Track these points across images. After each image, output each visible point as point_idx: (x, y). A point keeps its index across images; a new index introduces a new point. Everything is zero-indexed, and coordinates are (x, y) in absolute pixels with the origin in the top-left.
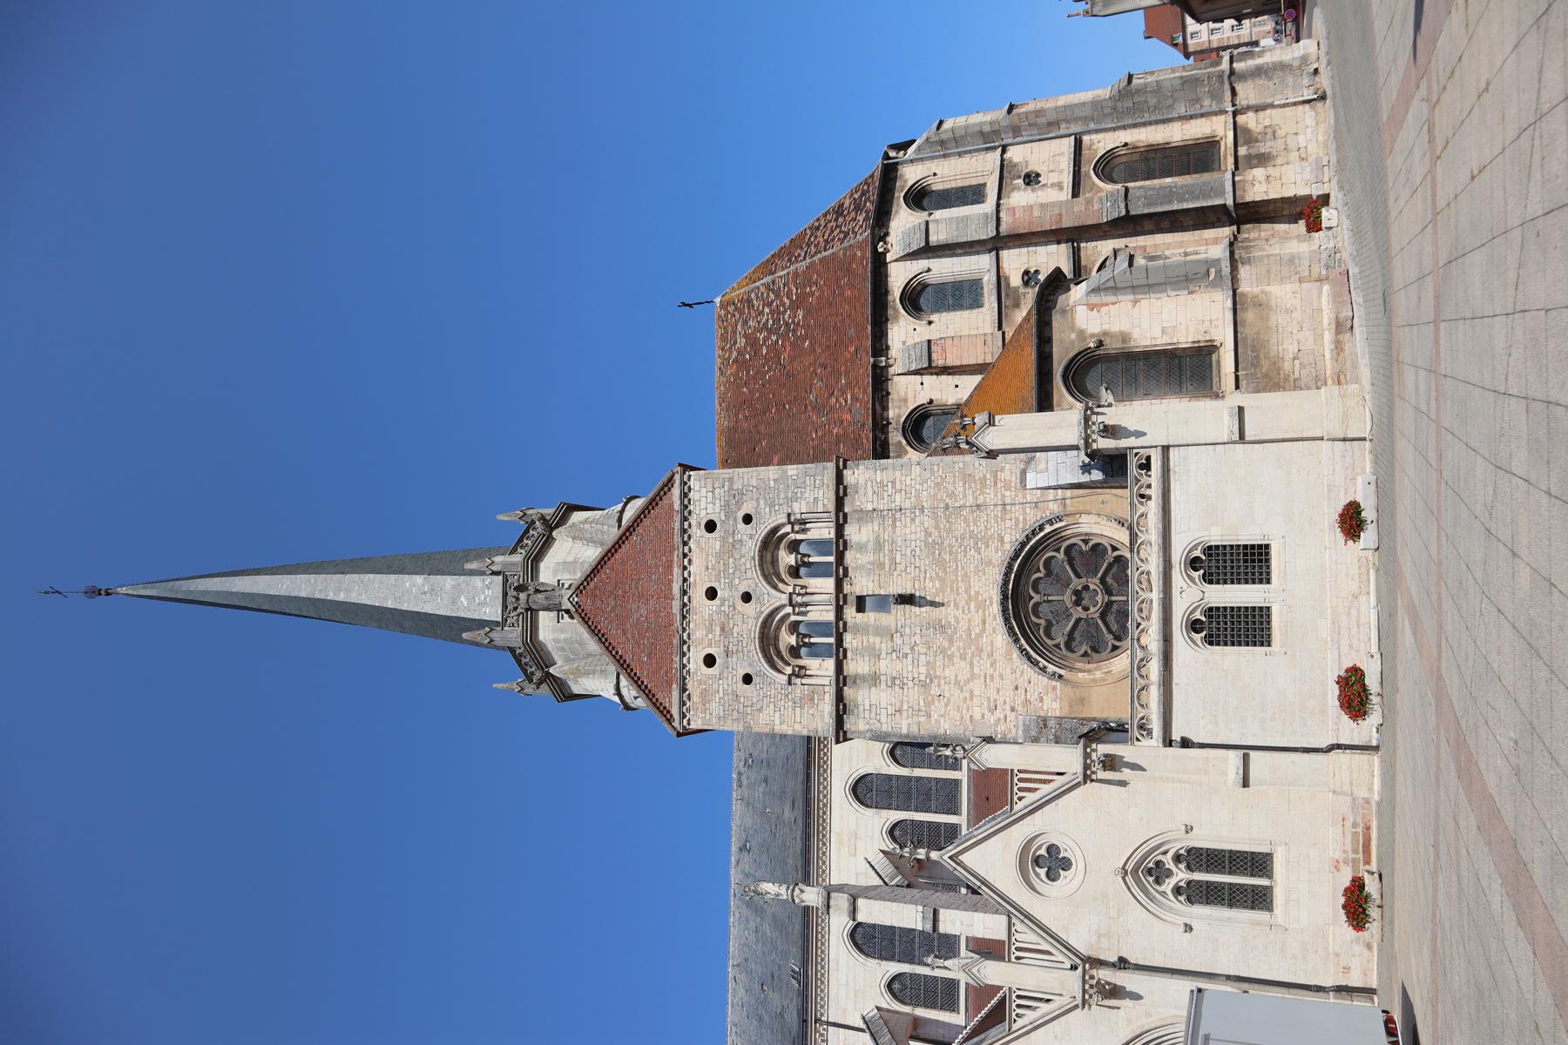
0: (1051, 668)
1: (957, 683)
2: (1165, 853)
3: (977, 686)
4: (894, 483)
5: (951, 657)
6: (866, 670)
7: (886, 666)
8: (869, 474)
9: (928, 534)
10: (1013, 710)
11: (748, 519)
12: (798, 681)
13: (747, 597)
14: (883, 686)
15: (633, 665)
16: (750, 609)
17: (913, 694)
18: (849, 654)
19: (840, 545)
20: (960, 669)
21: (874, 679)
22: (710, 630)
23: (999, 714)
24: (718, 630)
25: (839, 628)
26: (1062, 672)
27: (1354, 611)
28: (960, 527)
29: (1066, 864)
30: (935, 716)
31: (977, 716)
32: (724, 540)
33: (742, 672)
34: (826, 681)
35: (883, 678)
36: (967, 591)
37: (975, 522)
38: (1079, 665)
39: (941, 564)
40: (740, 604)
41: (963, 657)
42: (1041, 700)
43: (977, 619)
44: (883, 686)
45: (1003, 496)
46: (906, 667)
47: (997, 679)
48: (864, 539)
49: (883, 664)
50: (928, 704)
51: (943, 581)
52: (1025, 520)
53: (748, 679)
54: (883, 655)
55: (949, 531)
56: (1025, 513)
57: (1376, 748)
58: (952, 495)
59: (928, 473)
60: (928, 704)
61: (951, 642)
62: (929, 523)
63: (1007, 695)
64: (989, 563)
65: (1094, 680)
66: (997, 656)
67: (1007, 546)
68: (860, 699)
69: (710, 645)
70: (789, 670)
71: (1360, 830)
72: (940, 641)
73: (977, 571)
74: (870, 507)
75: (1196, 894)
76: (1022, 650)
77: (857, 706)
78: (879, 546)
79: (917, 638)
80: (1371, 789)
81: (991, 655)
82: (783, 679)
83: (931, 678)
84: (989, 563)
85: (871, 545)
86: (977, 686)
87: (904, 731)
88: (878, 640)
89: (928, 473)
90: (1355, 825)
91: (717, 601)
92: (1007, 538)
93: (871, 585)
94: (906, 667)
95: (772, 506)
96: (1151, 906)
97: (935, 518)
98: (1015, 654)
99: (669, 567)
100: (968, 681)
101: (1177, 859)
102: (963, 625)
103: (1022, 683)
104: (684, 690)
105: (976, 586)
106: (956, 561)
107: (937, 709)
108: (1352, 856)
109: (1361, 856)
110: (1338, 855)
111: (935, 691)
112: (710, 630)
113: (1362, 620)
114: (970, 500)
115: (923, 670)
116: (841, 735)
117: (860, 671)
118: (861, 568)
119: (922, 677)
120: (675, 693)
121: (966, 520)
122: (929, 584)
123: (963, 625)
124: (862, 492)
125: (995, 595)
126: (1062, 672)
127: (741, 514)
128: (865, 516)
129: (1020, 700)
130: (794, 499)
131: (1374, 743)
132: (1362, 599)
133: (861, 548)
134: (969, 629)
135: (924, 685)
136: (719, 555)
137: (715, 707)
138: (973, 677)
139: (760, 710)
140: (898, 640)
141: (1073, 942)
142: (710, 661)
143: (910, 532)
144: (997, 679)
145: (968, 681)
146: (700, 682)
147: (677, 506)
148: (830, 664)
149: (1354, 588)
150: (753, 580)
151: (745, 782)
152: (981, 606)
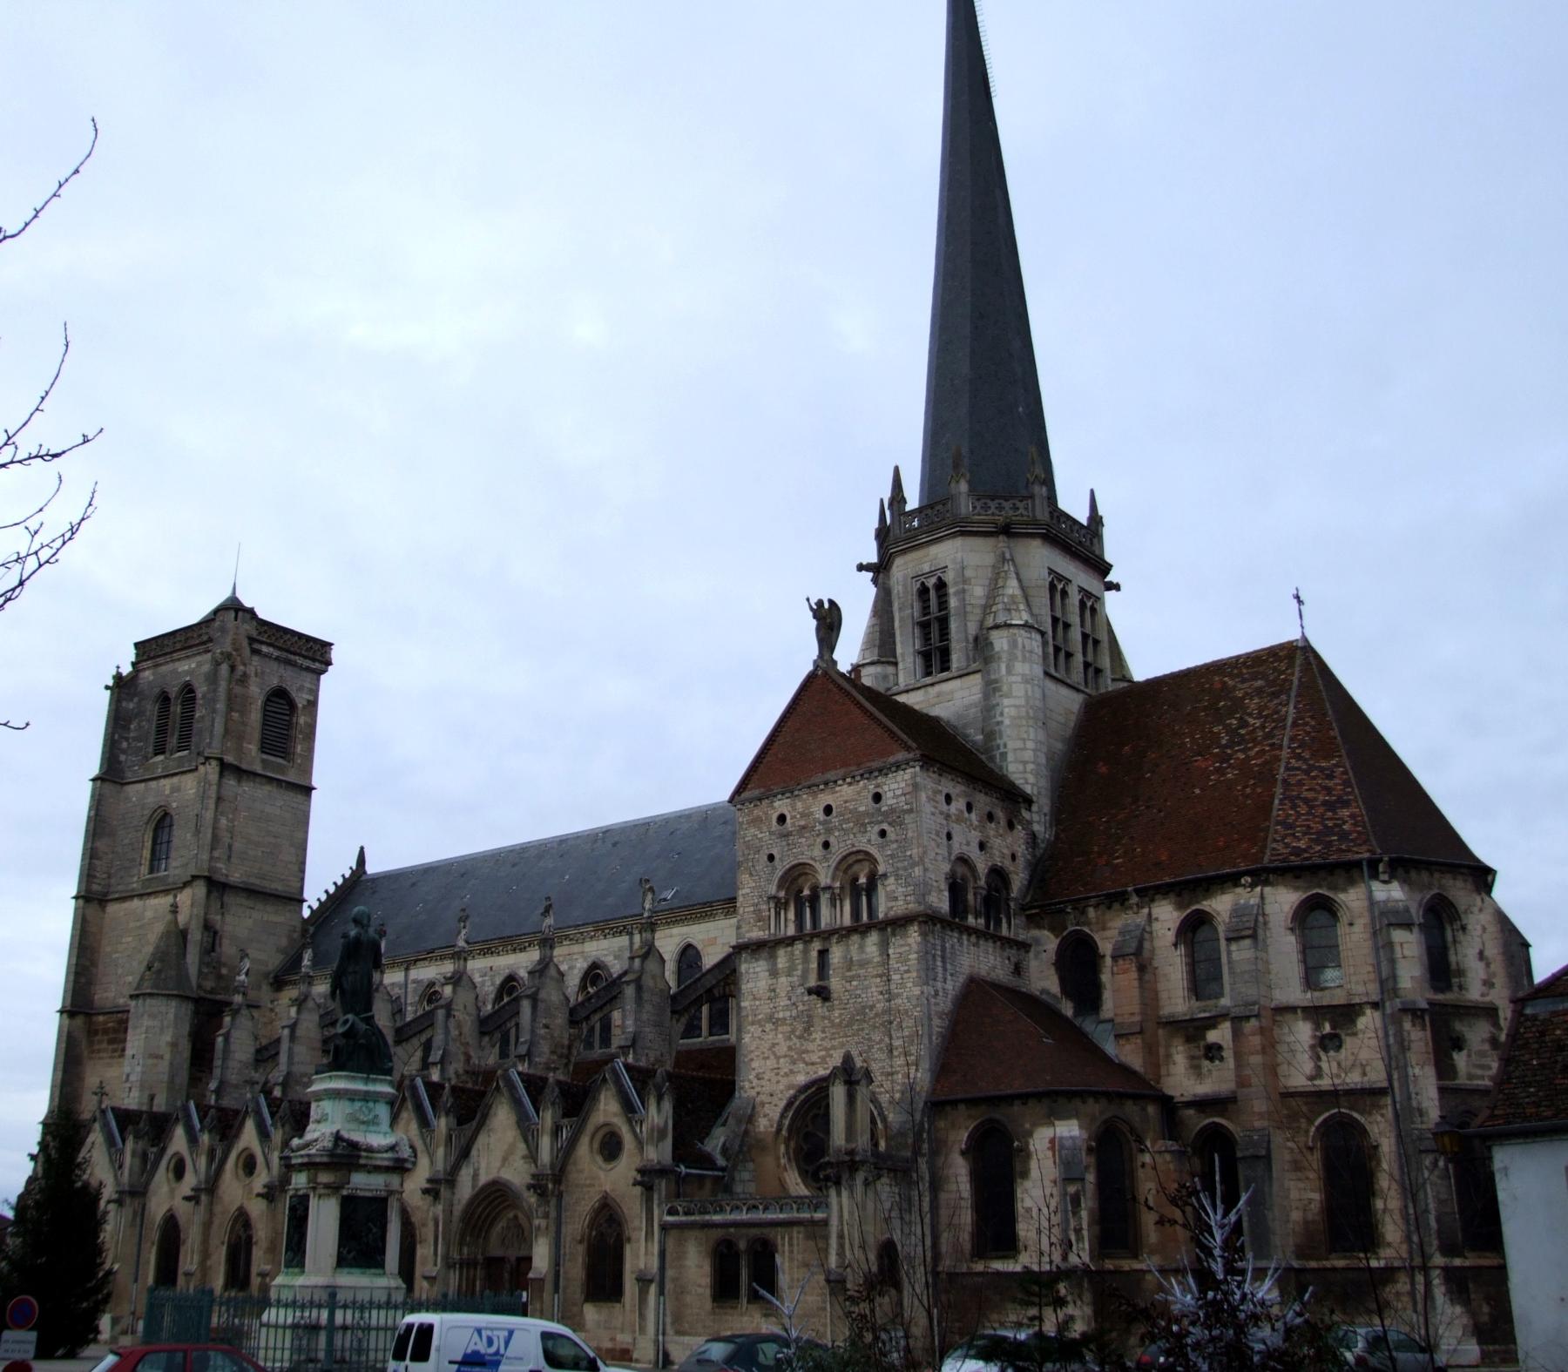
1: (774, 1045)
3: (771, 1063)
4: (908, 971)
5: (790, 1039)
9: (872, 1007)
11: (883, 834)
12: (772, 905)
13: (826, 845)
16: (818, 851)
17: (766, 1009)
21: (774, 973)
23: (755, 1082)
30: (752, 1029)
32: (866, 814)
33: (775, 852)
36: (834, 1048)
37: (880, 1049)
38: (792, 1144)
39: (850, 1025)
40: (820, 840)
41: (790, 1048)
43: (815, 1058)
49: (783, 980)
53: (771, 858)
60: (759, 1022)
61: (799, 1037)
62: (880, 1006)
63: (768, 1088)
65: (778, 1159)
66: (791, 1078)
70: (782, 894)
72: (800, 1028)
76: (795, 1097)
78: (863, 964)
79: (801, 1008)
81: (792, 1071)
82: (773, 890)
83: (776, 1023)
95: (892, 856)
97: (884, 1012)
98: (792, 1092)
102: (811, 1047)
103: (775, 1100)
111: (769, 1027)
112: (803, 815)
114: (896, 1043)
115: (781, 1015)
118: (848, 951)
121: (881, 1041)
123: (811, 1047)
128: (884, 946)
130: (898, 877)
133: (862, 948)
134: (807, 1052)
135: (770, 1018)
138: (778, 1058)
148: (791, 931)
150: (839, 849)
152: (823, 1059)
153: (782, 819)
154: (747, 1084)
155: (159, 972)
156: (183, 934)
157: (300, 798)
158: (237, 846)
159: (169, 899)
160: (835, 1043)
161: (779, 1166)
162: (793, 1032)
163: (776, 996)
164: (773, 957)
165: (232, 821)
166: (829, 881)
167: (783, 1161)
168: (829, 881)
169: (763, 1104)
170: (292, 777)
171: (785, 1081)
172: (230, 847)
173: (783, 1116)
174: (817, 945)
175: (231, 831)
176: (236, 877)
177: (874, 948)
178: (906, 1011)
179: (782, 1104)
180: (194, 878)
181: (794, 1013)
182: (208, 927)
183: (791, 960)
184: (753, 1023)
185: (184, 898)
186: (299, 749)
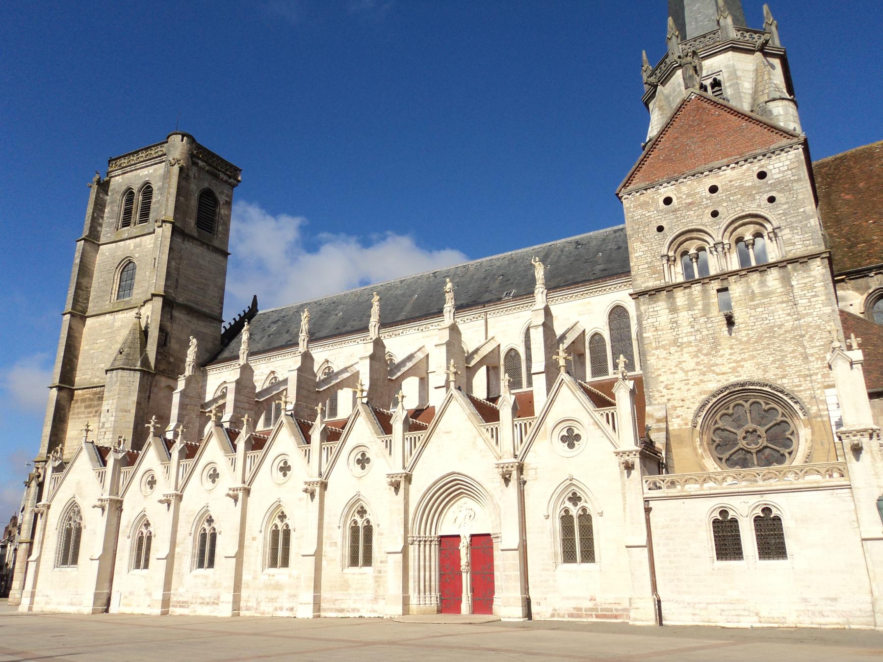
0: (700, 420)
1: (680, 363)
2: (586, 502)
5: (696, 356)
6: (678, 304)
7: (684, 316)
8: (820, 278)
9: (780, 327)
10: (669, 400)
12: (665, 261)
13: (715, 214)
14: (671, 316)
15: (656, 151)
17: (668, 336)
18: (687, 291)
19: (763, 267)
20: (690, 364)
21: (673, 309)
22: (688, 195)
23: (665, 392)
24: (690, 201)
25: (706, 279)
26: (698, 428)
27: (746, 613)
28: (788, 348)
29: (571, 446)
30: (657, 352)
31: (661, 379)
32: (753, 187)
33: (664, 224)
34: (667, 280)
35: (676, 315)
36: (744, 360)
38: (705, 437)
39: (760, 339)
40: (709, 211)
41: (698, 364)
42: (678, 417)
43: (725, 369)
44: (671, 316)
45: (817, 374)
46: (685, 329)
47: (687, 387)
48: (769, 284)
50: (664, 347)
51: (748, 342)
52: (800, 391)
53: (660, 229)
54: (690, 313)
55: (785, 341)
56: (805, 390)
57: (661, 624)
58: (812, 338)
59: (826, 319)
60: (664, 347)
61: (706, 355)
62: (789, 325)
63: (677, 395)
64: (765, 371)
65: (695, 449)
66: (702, 385)
67: (779, 382)
68: (660, 303)
69: (678, 198)
70: (671, 254)
71: (614, 612)
72: (706, 348)
73: (758, 364)
74: (793, 283)
75: (567, 519)
77: (655, 302)
78: (765, 295)
79: (705, 332)
80: (635, 620)
82: (664, 251)
83: (681, 346)
84: (765, 371)
85: (766, 289)
86: (680, 375)
87: (644, 335)
88: (700, 307)
89: (826, 319)
90: (617, 610)
91: (708, 194)
92: (785, 381)
93: (737, 295)
94: (685, 329)
95: (784, 214)
96: (555, 496)
97: (794, 329)
98: (704, 397)
99: (727, 155)
100: (682, 369)
101: (584, 509)
103: (687, 403)
104: (646, 190)
105: (748, 365)
106: (763, 349)
107: (662, 353)
108: (599, 608)
109: (600, 613)
110: (599, 600)
111: (673, 349)
112: (688, 195)
113: (741, 618)
114: (809, 351)
115: (685, 340)
116: (637, 295)
117: (678, 300)
118: (749, 287)
119: (680, 340)
120: (643, 185)
121: (794, 351)
122: (744, 333)
124: (805, 275)
125: (743, 378)
126: (698, 428)
127: (773, 194)
128: (786, 281)
129: (676, 403)
130: (792, 229)
131: (664, 622)
132: (756, 619)
133: (763, 283)
134: (717, 365)
135: (675, 342)
136: (741, 187)
137: (638, 213)
138: (686, 372)
139: (642, 242)
140: (702, 320)
141: (530, 455)
142: (668, 201)
143: (780, 314)
144: (687, 387)
145: (682, 369)
146: (653, 198)
147: (772, 147)
148: (680, 279)
149: (762, 614)
150: (727, 215)
151: (618, 234)
152: (734, 370)
153: (668, 201)
154: (657, 395)
155: (128, 354)
156: (145, 333)
157: (221, 258)
158: (181, 281)
159: (136, 311)
160: (747, 355)
161: (697, 454)
162: (700, 351)
163: (678, 327)
164: (671, 298)
165: (179, 264)
166: (720, 238)
167: (700, 451)
168: (720, 238)
169: (675, 408)
170: (216, 243)
171: (695, 390)
172: (177, 280)
173: (697, 415)
174: (715, 285)
175: (178, 270)
176: (180, 300)
177: (777, 282)
178: (819, 327)
179: (697, 405)
180: (153, 295)
181: (699, 337)
182: (162, 329)
183: (690, 298)
184: (657, 348)
185: (146, 311)
186: (220, 228)
